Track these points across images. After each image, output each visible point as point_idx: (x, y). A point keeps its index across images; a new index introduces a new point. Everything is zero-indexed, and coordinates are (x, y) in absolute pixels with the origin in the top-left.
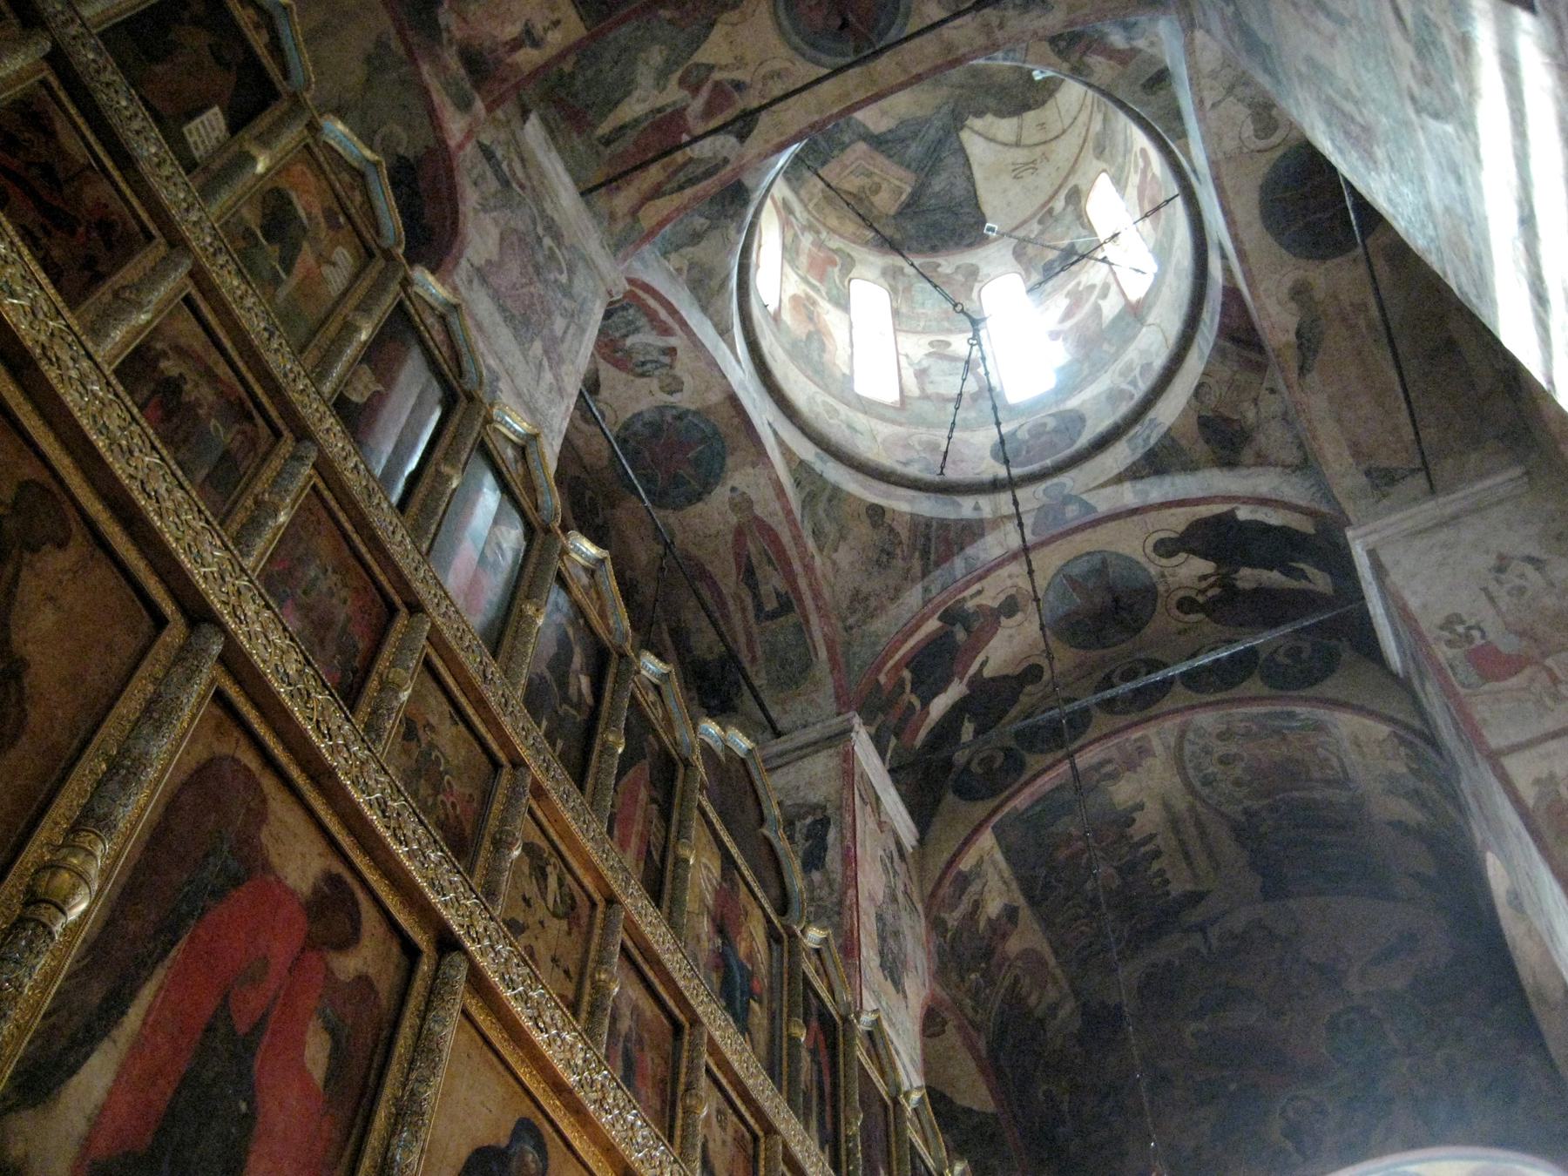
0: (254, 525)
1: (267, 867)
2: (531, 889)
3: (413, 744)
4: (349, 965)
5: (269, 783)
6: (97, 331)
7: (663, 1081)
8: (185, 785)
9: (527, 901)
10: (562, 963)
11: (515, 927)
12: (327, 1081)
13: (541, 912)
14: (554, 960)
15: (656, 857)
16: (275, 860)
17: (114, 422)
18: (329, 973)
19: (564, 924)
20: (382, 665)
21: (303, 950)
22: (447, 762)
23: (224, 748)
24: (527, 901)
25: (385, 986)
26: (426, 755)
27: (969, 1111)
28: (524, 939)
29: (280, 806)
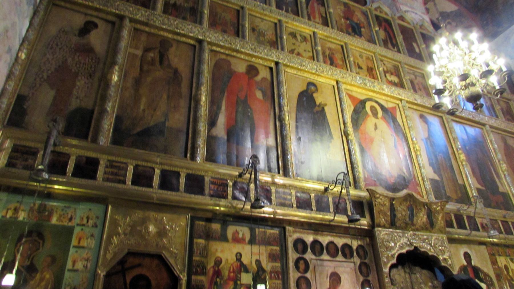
0: (201, 17)
1: (235, 72)
2: (294, 41)
3: (255, 32)
4: (259, 78)
5: (229, 58)
6: (154, 9)
7: (342, 58)
8: (213, 69)
9: (294, 44)
10: (307, 50)
11: (292, 52)
12: (263, 98)
13: (297, 44)
14: (305, 51)
15: (324, 15)
16: (236, 70)
17: (166, 21)
18: (255, 81)
19: (305, 43)
20: (240, 22)
21: (249, 80)
22: (264, 30)
23: (218, 58)
24: (294, 44)
25: (268, 77)
26: (259, 32)
27: (452, 12)
28: (296, 52)
29: (232, 61)
